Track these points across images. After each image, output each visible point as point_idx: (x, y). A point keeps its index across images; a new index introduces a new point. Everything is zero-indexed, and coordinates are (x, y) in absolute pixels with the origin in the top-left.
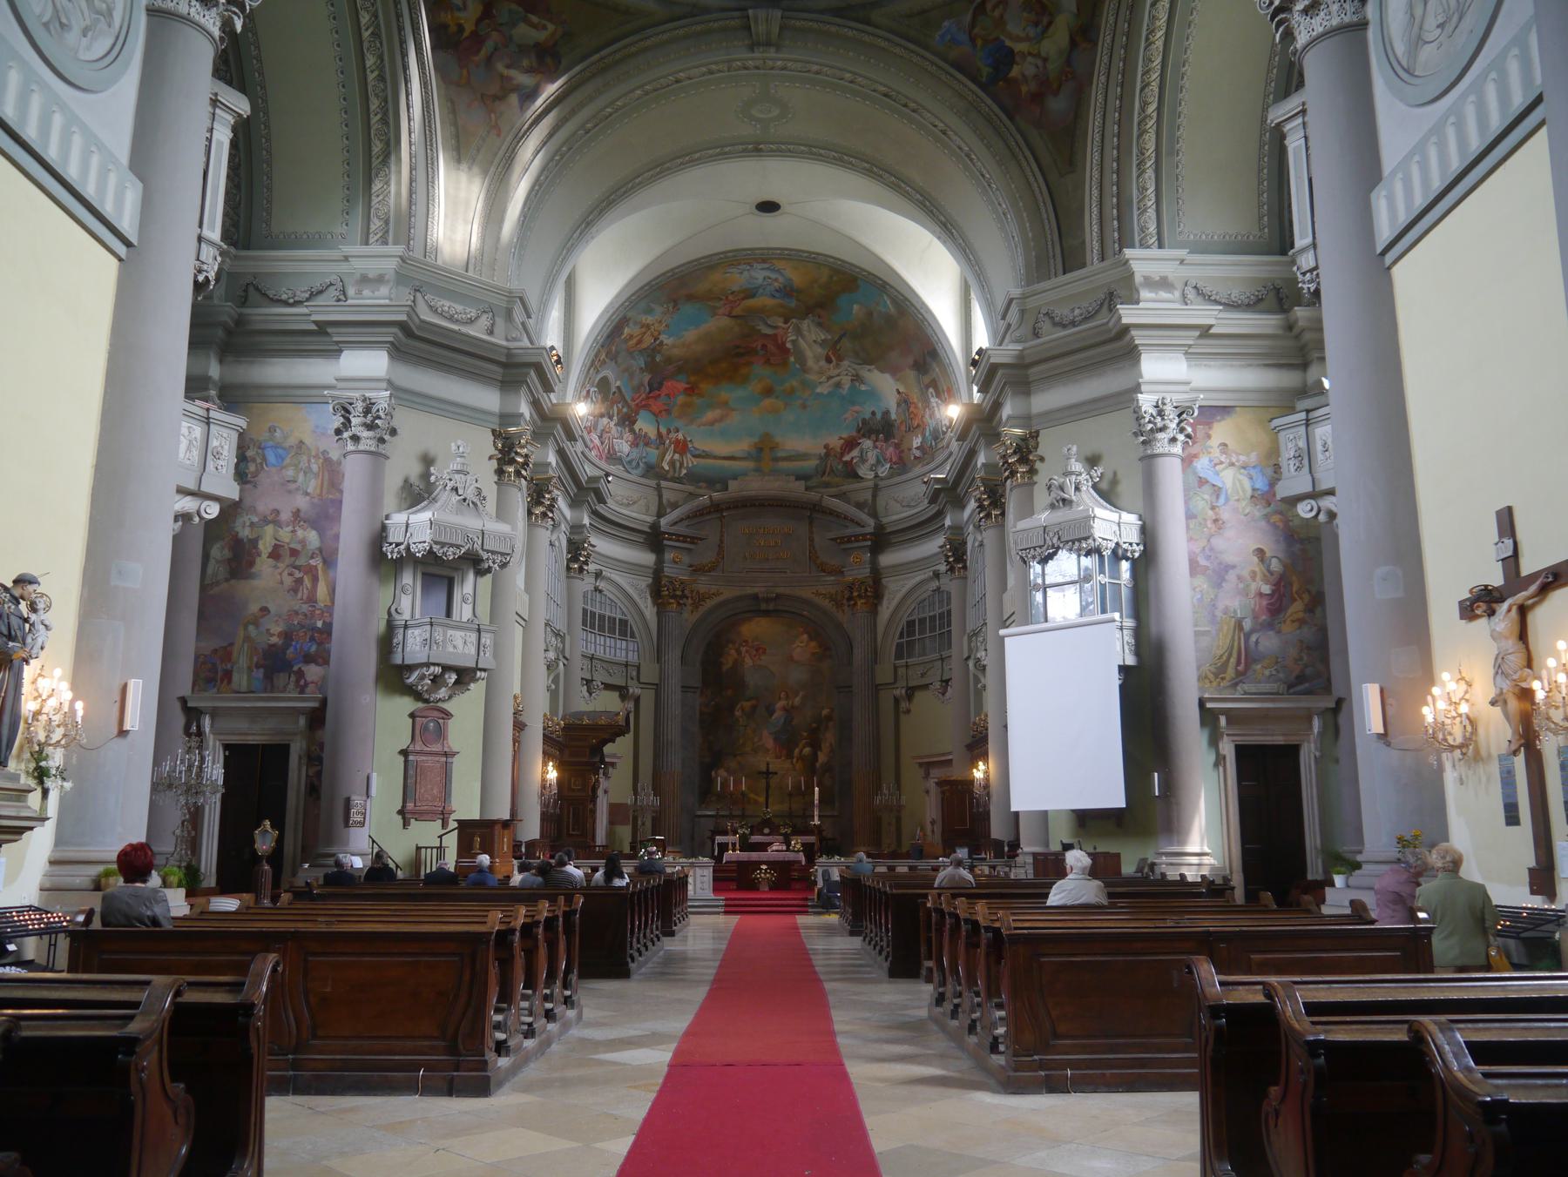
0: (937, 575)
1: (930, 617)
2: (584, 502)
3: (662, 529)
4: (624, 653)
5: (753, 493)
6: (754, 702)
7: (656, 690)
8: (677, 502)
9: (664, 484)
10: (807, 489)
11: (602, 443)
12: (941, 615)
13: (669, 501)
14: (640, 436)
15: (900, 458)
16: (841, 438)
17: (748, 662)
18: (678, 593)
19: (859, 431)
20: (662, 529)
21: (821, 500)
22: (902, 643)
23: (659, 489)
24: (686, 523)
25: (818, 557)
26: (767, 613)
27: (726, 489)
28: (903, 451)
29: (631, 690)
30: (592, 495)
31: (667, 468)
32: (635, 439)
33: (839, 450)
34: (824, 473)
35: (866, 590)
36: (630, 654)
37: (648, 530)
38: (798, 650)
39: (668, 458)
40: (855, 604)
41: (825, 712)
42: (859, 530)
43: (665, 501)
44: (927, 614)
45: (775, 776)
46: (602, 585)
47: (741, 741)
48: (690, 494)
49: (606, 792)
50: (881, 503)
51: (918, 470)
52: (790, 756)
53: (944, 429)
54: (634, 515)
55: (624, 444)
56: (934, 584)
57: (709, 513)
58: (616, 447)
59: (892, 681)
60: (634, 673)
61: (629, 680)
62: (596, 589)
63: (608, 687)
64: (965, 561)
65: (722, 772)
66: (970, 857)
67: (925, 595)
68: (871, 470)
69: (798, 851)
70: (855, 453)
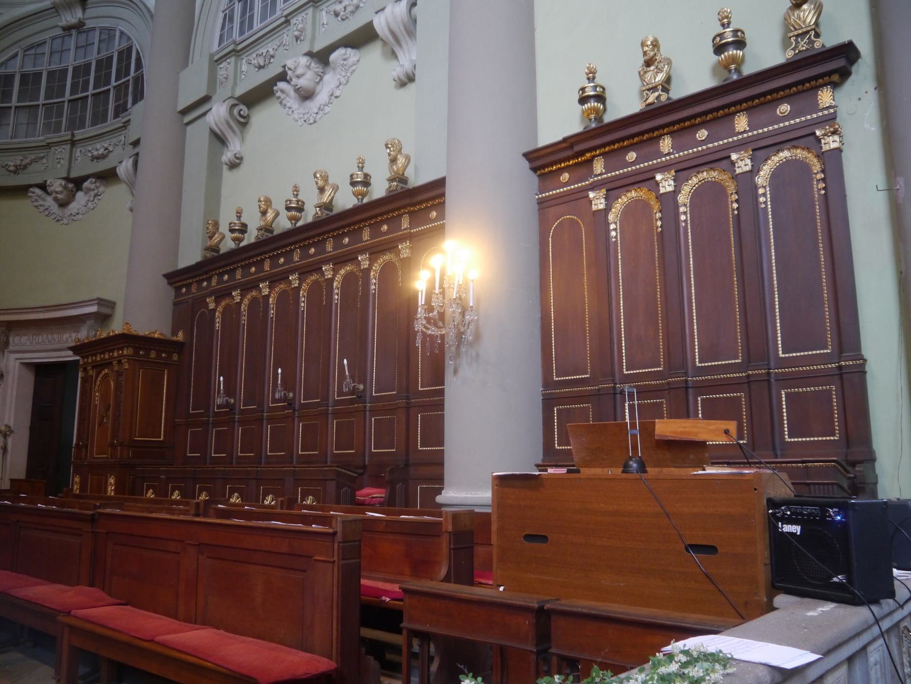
1: (51, 74)
44: (44, 66)
67: (47, 36)
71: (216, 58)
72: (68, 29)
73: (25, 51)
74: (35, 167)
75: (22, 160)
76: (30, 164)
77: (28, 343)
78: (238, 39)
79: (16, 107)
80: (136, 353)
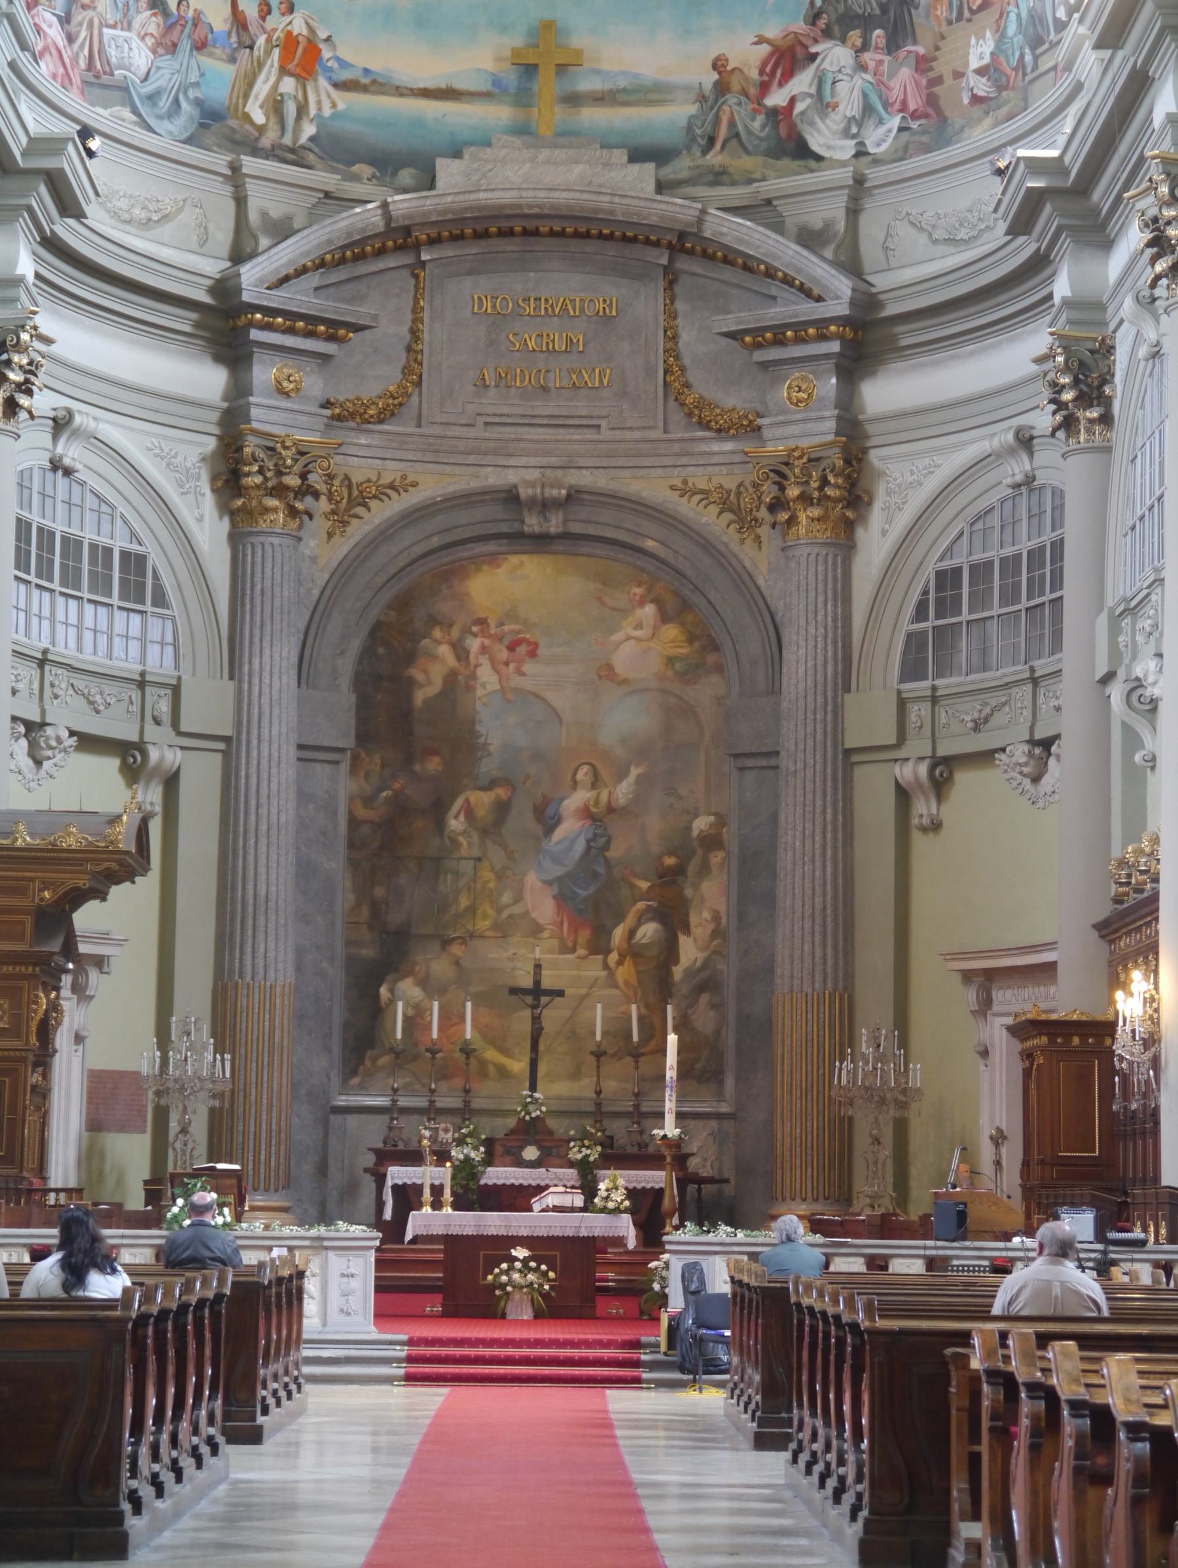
0: (1026, 442)
1: (1003, 561)
2: (17, 208)
3: (246, 297)
4: (134, 647)
5: (506, 197)
6: (501, 792)
7: (226, 754)
8: (289, 218)
9: (250, 164)
10: (661, 187)
11: (71, 39)
12: (1036, 556)
13: (264, 215)
14: (180, 21)
15: (932, 101)
16: (761, 40)
17: (486, 676)
18: (293, 481)
19: (814, 17)
20: (246, 297)
21: (700, 221)
22: (924, 633)
23: (235, 177)
24: (314, 279)
25: (687, 385)
26: (541, 542)
27: (430, 183)
28: (939, 80)
29: (154, 754)
30: (43, 189)
31: (259, 118)
32: (169, 28)
33: (754, 74)
34: (711, 141)
35: (824, 482)
36: (153, 651)
37: (207, 299)
38: (628, 649)
39: (262, 88)
40: (792, 521)
41: (701, 824)
42: (806, 310)
43: (253, 217)
44: (994, 554)
45: (558, 1000)
46: (71, 452)
47: (464, 902)
48: (327, 195)
49: (79, 1039)
50: (871, 229)
51: (980, 135)
52: (599, 946)
53: (1061, 14)
54: (165, 253)
55: (136, 42)
56: (1018, 467)
57: (381, 252)
58: (112, 53)
59: (892, 740)
60: (164, 707)
61: (150, 726)
62: (56, 465)
63: (88, 742)
64: (1107, 402)
65: (409, 989)
66: (1100, 1236)
67: (993, 498)
68: (846, 134)
69: (617, 1211)
70: (802, 82)
71: (1118, 612)
72: (1017, 486)
73: (972, 525)
74: (999, 719)
75: (980, 711)
76: (992, 715)
77: (1014, 1001)
78: (1129, 594)
79: (968, 622)
80: (1052, 1040)
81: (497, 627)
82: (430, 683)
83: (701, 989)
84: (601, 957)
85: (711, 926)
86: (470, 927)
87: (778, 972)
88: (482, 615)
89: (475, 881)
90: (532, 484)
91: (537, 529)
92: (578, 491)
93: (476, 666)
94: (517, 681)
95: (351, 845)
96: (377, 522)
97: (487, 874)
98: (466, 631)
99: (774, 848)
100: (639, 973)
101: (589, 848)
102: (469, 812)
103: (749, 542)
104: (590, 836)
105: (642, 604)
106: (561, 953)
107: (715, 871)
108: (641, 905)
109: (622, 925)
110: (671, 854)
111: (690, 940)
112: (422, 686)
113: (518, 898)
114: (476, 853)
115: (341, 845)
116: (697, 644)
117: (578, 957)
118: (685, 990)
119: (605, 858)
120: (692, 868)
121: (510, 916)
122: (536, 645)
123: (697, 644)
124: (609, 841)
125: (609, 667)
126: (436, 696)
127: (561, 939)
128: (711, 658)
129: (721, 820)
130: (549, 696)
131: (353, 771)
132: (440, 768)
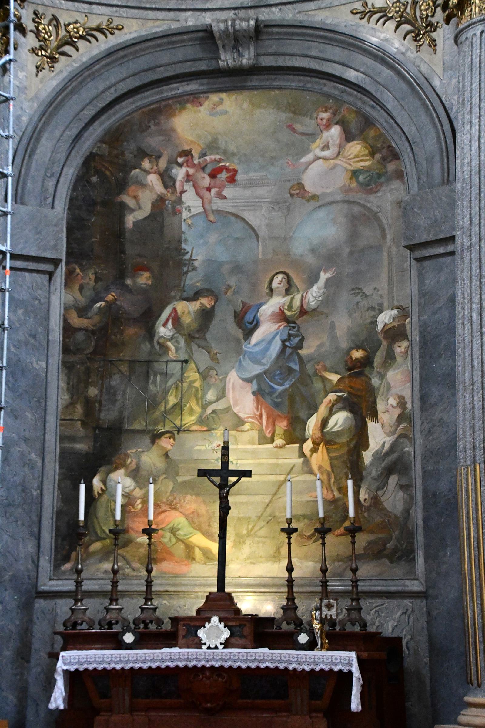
6: (205, 302)
47: (172, 400)
81: (200, 158)
82: (140, 208)
83: (389, 471)
84: (297, 445)
85: (398, 411)
86: (178, 423)
87: (460, 445)
88: (187, 148)
89: (182, 381)
90: (226, 21)
91: (231, 63)
92: (266, 26)
93: (182, 192)
94: (218, 204)
95: (66, 350)
96: (84, 60)
97: (192, 375)
98: (173, 162)
99: (452, 330)
100: (331, 458)
101: (284, 347)
102: (176, 320)
103: (425, 47)
104: (285, 337)
105: (328, 126)
106: (259, 444)
107: (399, 359)
108: (332, 396)
109: (315, 416)
110: (357, 348)
111: (378, 425)
112: (132, 210)
113: (222, 395)
114: (182, 356)
115: (56, 350)
116: (378, 156)
117: (277, 447)
118: (374, 473)
119: (299, 355)
120: (377, 360)
121: (214, 412)
122: (235, 171)
123: (378, 156)
124: (302, 339)
125: (300, 186)
126: (145, 219)
127: (261, 431)
128: (391, 167)
129: (404, 313)
130: (247, 215)
131: (69, 282)
132: (150, 282)
